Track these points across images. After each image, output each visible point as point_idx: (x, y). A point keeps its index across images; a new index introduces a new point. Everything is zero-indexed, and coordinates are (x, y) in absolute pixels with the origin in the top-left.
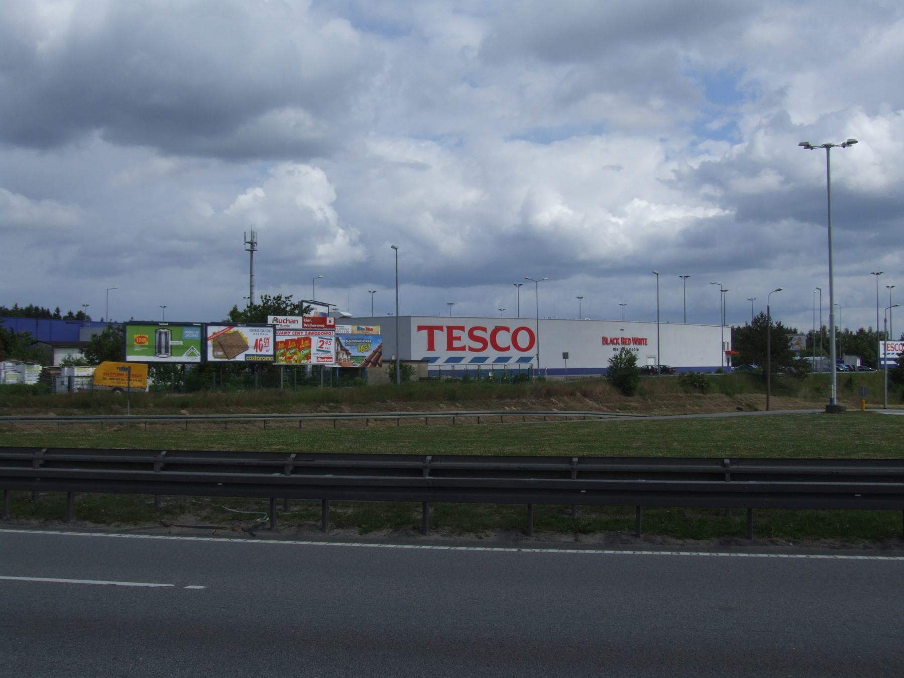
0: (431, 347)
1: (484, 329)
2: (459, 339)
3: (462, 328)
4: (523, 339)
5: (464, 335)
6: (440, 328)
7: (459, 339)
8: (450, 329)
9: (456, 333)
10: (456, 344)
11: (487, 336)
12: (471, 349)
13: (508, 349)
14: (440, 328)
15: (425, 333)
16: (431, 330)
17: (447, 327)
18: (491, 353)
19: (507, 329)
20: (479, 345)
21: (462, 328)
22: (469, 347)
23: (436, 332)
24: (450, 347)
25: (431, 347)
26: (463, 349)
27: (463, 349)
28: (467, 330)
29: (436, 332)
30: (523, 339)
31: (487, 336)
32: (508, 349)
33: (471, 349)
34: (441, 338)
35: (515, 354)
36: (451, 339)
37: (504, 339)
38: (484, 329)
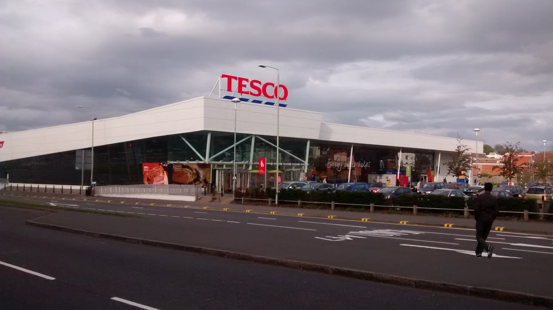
0: (229, 89)
1: (260, 83)
2: (245, 86)
3: (247, 80)
5: (248, 84)
6: (235, 78)
7: (245, 86)
8: (241, 80)
9: (244, 82)
11: (261, 87)
12: (251, 94)
13: (272, 97)
14: (235, 78)
15: (226, 79)
16: (230, 78)
18: (262, 98)
20: (256, 92)
21: (247, 80)
22: (250, 92)
24: (240, 91)
25: (229, 89)
29: (233, 80)
31: (261, 87)
32: (272, 97)
33: (251, 94)
36: (240, 86)
38: (260, 83)
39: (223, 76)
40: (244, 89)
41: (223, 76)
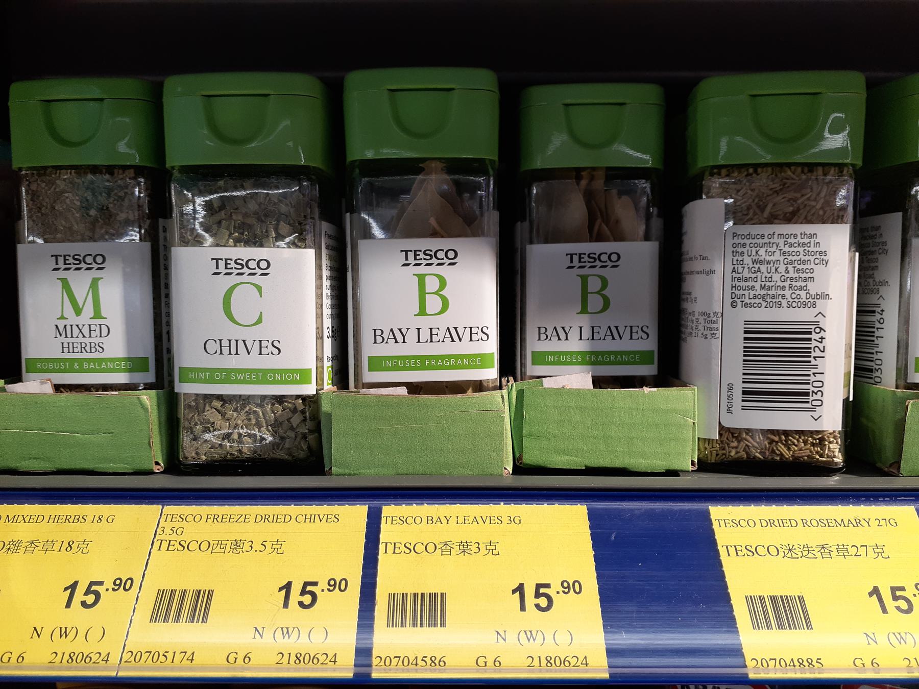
0: (217, 268)
1: (242, 260)
2: (230, 264)
3: (231, 260)
4: (263, 265)
5: (232, 263)
6: (222, 259)
7: (230, 264)
8: (226, 260)
10: (229, 266)
12: (236, 268)
14: (222, 259)
16: (217, 260)
17: (225, 259)
18: (245, 270)
19: (254, 260)
20: (240, 267)
21: (231, 260)
23: (219, 261)
24: (226, 268)
25: (217, 268)
26: (232, 268)
27: (232, 268)
28: (234, 260)
30: (263, 265)
32: (255, 269)
33: (236, 268)
34: (222, 264)
35: (258, 271)
36: (226, 264)
37: (252, 264)
38: (242, 260)
39: (212, 259)
40: (229, 266)
41: (212, 259)
